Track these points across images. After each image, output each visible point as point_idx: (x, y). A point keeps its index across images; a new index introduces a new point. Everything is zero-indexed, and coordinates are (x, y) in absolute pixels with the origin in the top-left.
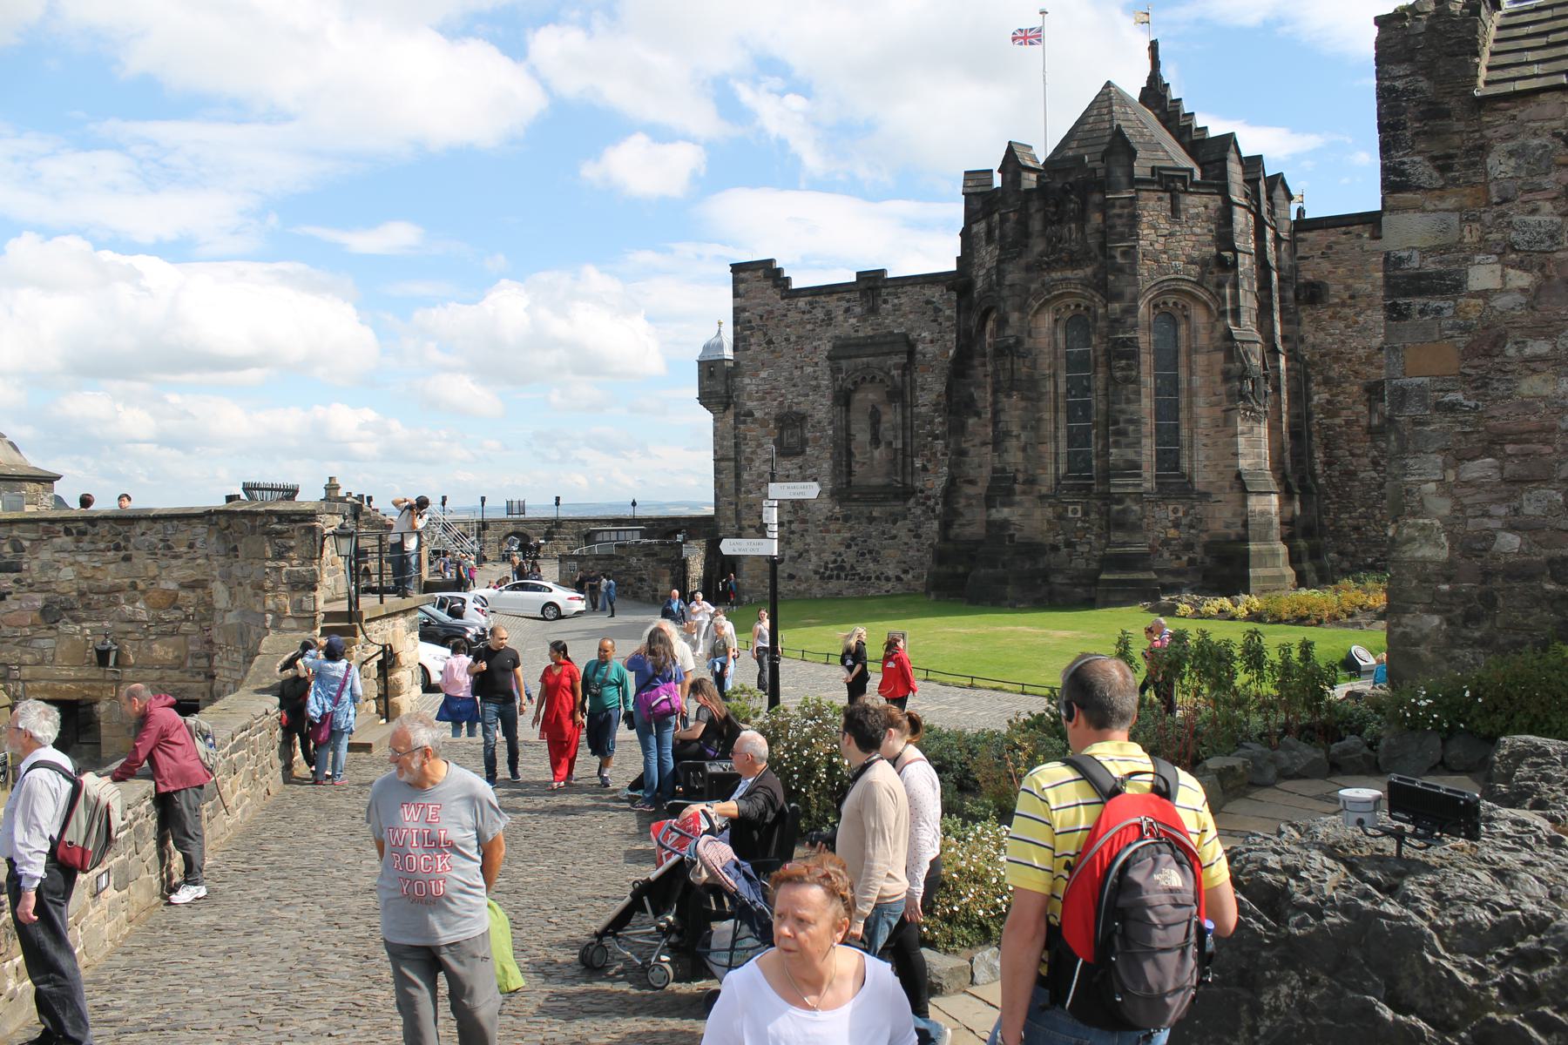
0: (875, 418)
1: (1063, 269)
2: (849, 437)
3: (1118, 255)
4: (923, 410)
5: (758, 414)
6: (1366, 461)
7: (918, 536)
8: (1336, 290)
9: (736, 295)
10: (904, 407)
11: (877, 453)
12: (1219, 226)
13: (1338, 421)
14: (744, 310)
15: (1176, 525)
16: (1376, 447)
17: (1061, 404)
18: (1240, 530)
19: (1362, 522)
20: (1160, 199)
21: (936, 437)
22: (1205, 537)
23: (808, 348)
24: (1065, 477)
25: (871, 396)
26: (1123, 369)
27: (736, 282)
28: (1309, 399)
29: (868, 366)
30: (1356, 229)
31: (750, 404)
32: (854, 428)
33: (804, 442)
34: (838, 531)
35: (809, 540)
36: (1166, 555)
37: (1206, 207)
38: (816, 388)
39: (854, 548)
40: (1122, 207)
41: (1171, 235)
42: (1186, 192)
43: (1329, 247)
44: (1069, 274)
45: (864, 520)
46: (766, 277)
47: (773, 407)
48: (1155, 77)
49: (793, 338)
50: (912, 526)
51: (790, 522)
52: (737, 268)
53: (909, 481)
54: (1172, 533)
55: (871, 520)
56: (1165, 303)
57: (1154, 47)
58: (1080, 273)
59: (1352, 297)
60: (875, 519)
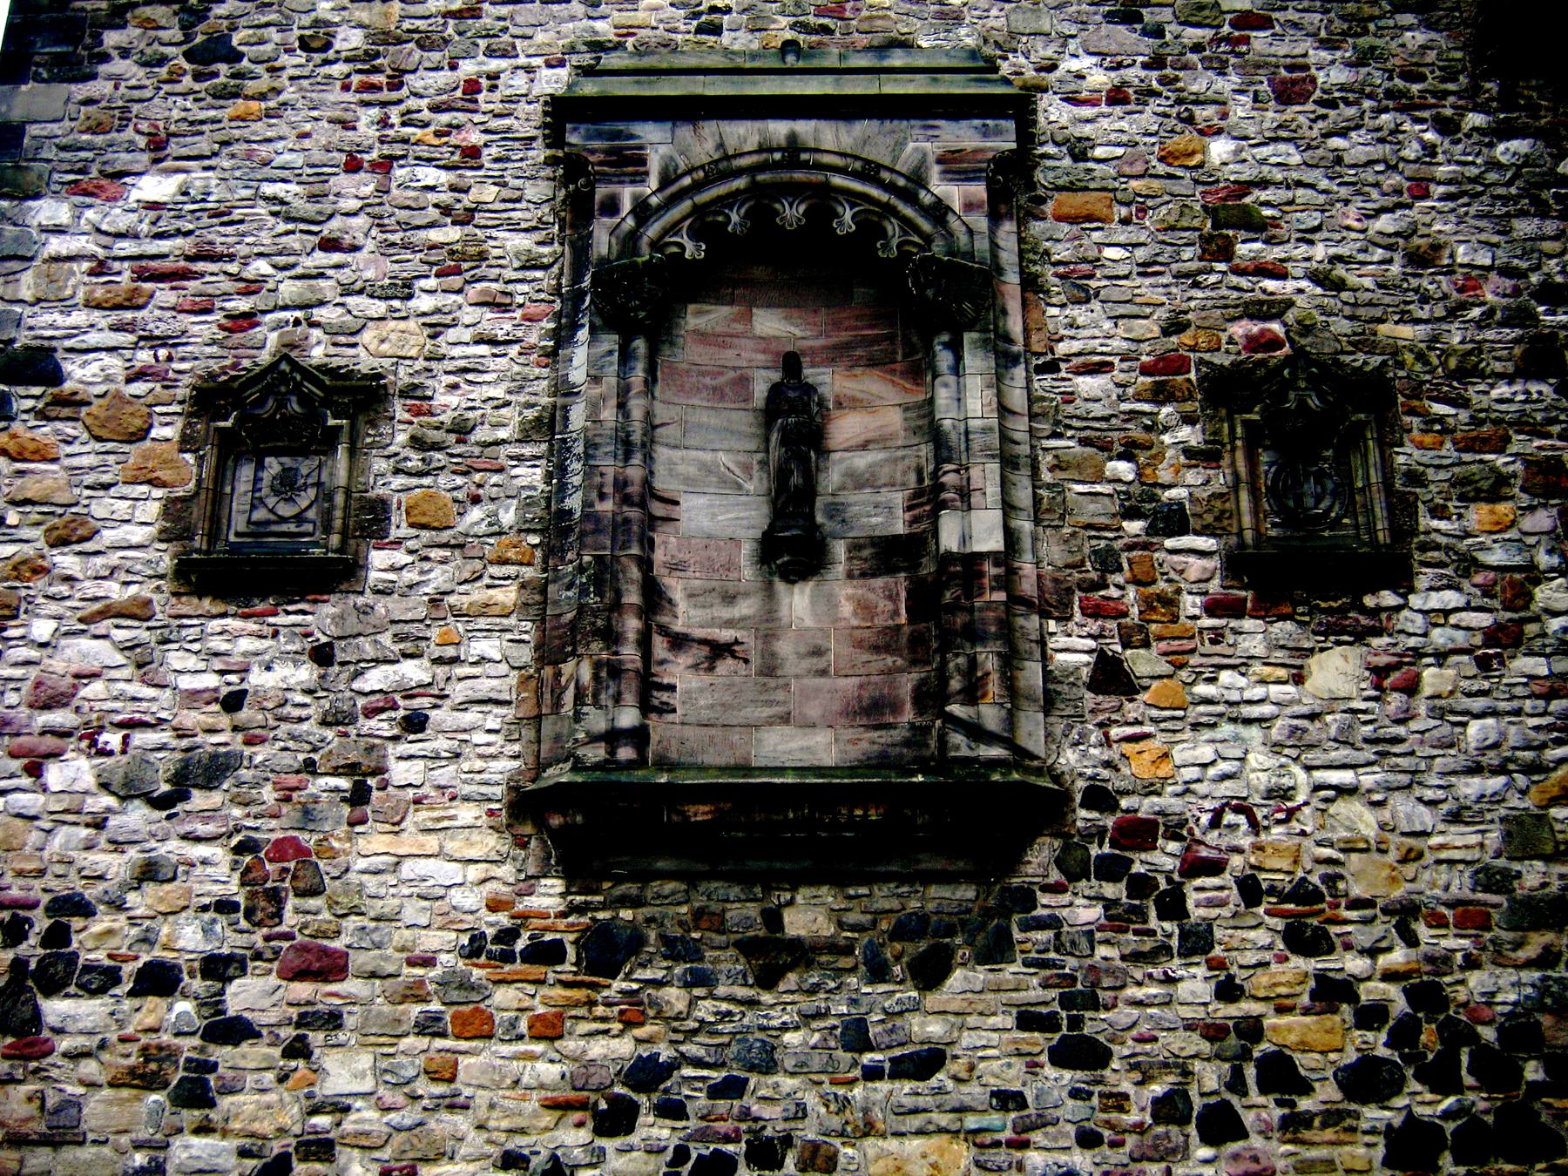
0: (794, 425)
2: (646, 509)
4: (1087, 385)
5: (80, 373)
7: (1082, 1053)
10: (1005, 360)
11: (798, 602)
21: (1173, 521)
23: (429, 82)
25: (771, 324)
29: (793, 146)
31: (48, 322)
32: (673, 466)
33: (371, 520)
34: (549, 1030)
35: (345, 1070)
38: (458, 265)
39: (653, 1129)
45: (726, 962)
47: (202, 346)
49: (350, 39)
50: (1034, 992)
51: (219, 968)
53: (1032, 731)
55: (772, 957)
60: (802, 953)
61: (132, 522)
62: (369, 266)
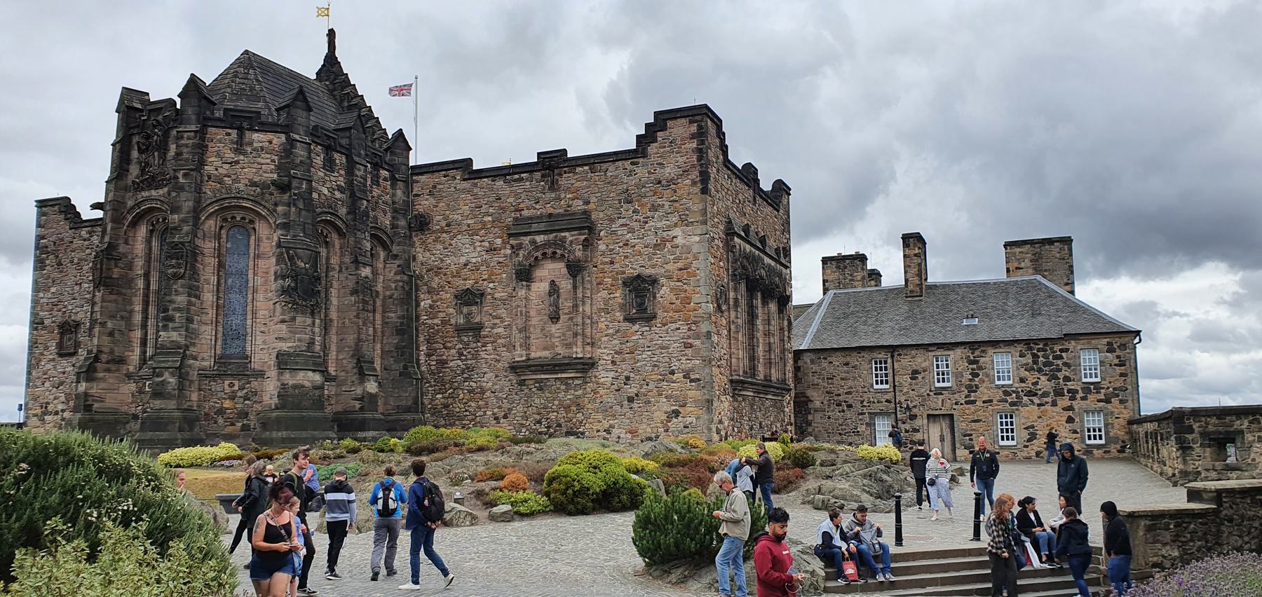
1: (149, 188)
3: (180, 175)
5: (47, 322)
6: (453, 351)
8: (438, 221)
9: (39, 225)
12: (281, 158)
13: (436, 321)
14: (43, 238)
15: (232, 397)
16: (461, 341)
17: (152, 298)
18: (276, 400)
19: (450, 401)
20: (228, 134)
22: (258, 407)
24: (151, 358)
26: (174, 267)
27: (41, 214)
28: (418, 305)
30: (452, 173)
36: (221, 421)
37: (270, 142)
40: (189, 138)
41: (237, 162)
42: (251, 129)
43: (435, 187)
44: (153, 193)
46: (61, 212)
47: (59, 320)
48: (331, 61)
49: (76, 261)
51: (63, 411)
52: (42, 204)
54: (227, 404)
56: (234, 218)
57: (331, 34)
58: (161, 192)
59: (448, 225)
61: (53, 346)
62: (78, 302)
